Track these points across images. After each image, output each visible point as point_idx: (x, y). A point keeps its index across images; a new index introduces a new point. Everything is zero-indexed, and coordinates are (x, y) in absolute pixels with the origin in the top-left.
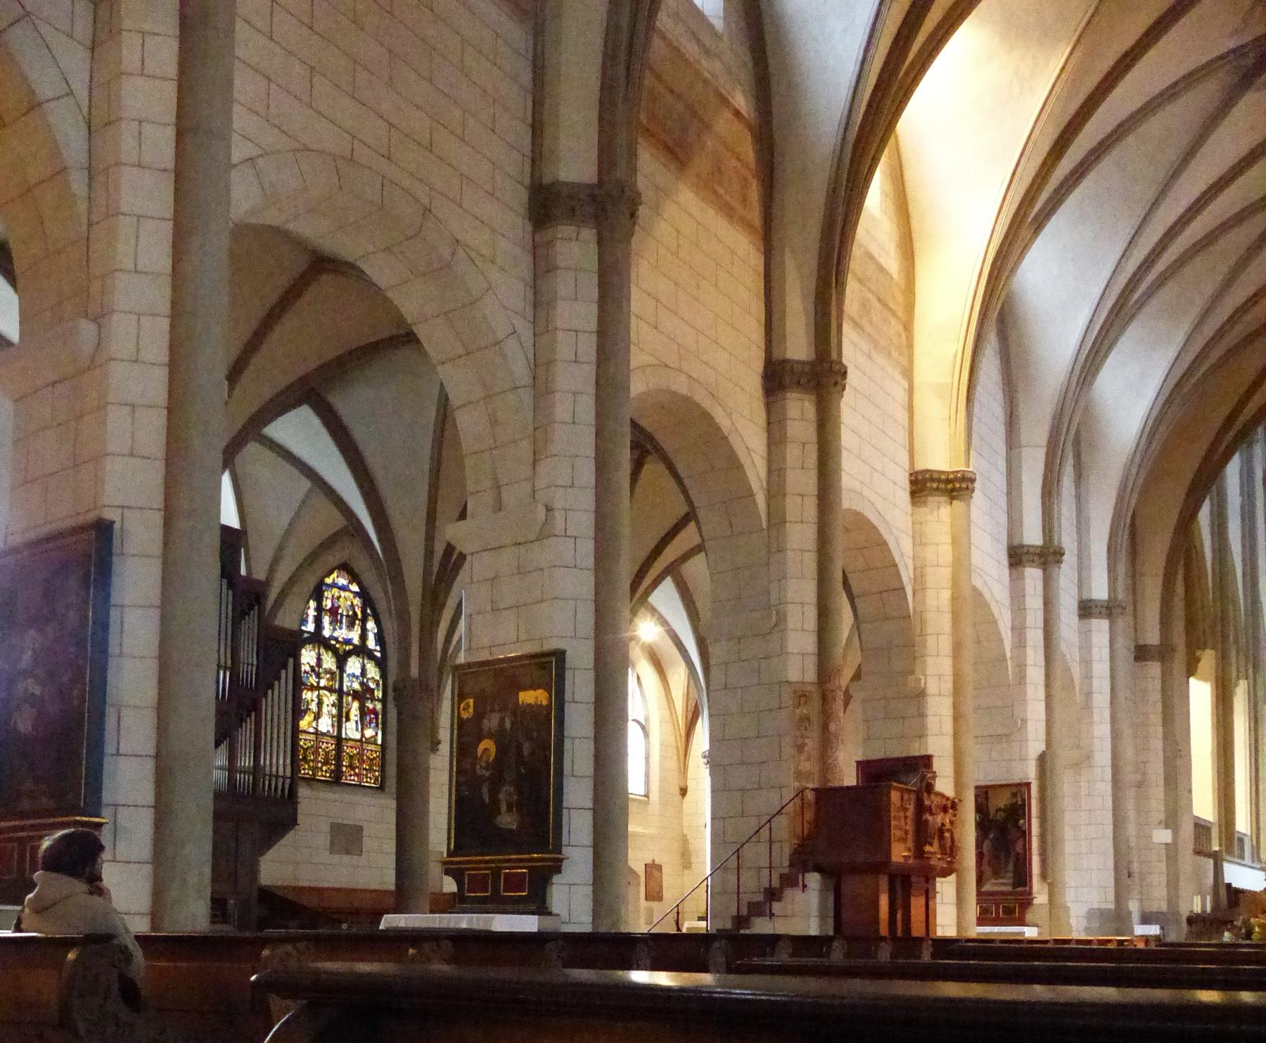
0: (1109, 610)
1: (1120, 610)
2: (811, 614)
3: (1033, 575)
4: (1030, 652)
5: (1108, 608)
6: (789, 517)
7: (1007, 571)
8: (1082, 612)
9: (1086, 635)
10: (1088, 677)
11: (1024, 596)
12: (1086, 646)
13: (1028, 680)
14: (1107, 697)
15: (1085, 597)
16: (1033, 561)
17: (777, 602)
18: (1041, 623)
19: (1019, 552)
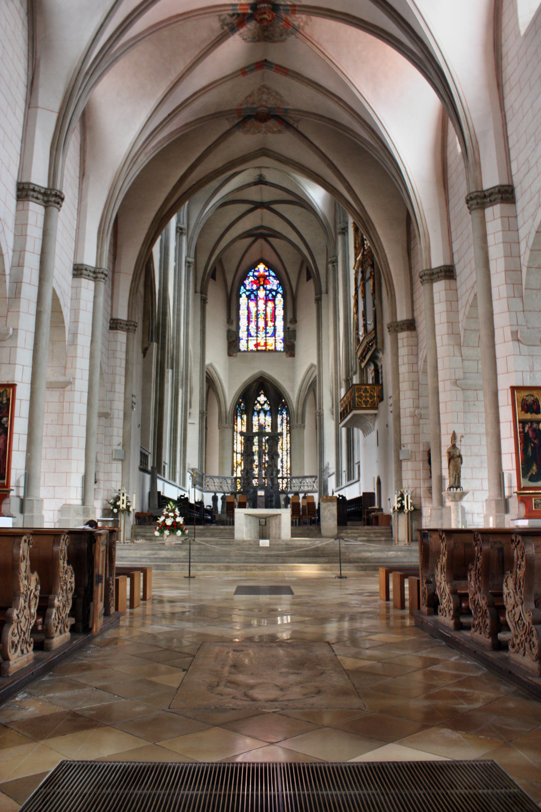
1: (103, 276)
4: (26, 271)
5: (94, 272)
7: (14, 201)
8: (75, 272)
9: (76, 290)
10: (76, 321)
11: (27, 224)
12: (76, 298)
15: (79, 262)
16: (37, 198)
18: (38, 250)
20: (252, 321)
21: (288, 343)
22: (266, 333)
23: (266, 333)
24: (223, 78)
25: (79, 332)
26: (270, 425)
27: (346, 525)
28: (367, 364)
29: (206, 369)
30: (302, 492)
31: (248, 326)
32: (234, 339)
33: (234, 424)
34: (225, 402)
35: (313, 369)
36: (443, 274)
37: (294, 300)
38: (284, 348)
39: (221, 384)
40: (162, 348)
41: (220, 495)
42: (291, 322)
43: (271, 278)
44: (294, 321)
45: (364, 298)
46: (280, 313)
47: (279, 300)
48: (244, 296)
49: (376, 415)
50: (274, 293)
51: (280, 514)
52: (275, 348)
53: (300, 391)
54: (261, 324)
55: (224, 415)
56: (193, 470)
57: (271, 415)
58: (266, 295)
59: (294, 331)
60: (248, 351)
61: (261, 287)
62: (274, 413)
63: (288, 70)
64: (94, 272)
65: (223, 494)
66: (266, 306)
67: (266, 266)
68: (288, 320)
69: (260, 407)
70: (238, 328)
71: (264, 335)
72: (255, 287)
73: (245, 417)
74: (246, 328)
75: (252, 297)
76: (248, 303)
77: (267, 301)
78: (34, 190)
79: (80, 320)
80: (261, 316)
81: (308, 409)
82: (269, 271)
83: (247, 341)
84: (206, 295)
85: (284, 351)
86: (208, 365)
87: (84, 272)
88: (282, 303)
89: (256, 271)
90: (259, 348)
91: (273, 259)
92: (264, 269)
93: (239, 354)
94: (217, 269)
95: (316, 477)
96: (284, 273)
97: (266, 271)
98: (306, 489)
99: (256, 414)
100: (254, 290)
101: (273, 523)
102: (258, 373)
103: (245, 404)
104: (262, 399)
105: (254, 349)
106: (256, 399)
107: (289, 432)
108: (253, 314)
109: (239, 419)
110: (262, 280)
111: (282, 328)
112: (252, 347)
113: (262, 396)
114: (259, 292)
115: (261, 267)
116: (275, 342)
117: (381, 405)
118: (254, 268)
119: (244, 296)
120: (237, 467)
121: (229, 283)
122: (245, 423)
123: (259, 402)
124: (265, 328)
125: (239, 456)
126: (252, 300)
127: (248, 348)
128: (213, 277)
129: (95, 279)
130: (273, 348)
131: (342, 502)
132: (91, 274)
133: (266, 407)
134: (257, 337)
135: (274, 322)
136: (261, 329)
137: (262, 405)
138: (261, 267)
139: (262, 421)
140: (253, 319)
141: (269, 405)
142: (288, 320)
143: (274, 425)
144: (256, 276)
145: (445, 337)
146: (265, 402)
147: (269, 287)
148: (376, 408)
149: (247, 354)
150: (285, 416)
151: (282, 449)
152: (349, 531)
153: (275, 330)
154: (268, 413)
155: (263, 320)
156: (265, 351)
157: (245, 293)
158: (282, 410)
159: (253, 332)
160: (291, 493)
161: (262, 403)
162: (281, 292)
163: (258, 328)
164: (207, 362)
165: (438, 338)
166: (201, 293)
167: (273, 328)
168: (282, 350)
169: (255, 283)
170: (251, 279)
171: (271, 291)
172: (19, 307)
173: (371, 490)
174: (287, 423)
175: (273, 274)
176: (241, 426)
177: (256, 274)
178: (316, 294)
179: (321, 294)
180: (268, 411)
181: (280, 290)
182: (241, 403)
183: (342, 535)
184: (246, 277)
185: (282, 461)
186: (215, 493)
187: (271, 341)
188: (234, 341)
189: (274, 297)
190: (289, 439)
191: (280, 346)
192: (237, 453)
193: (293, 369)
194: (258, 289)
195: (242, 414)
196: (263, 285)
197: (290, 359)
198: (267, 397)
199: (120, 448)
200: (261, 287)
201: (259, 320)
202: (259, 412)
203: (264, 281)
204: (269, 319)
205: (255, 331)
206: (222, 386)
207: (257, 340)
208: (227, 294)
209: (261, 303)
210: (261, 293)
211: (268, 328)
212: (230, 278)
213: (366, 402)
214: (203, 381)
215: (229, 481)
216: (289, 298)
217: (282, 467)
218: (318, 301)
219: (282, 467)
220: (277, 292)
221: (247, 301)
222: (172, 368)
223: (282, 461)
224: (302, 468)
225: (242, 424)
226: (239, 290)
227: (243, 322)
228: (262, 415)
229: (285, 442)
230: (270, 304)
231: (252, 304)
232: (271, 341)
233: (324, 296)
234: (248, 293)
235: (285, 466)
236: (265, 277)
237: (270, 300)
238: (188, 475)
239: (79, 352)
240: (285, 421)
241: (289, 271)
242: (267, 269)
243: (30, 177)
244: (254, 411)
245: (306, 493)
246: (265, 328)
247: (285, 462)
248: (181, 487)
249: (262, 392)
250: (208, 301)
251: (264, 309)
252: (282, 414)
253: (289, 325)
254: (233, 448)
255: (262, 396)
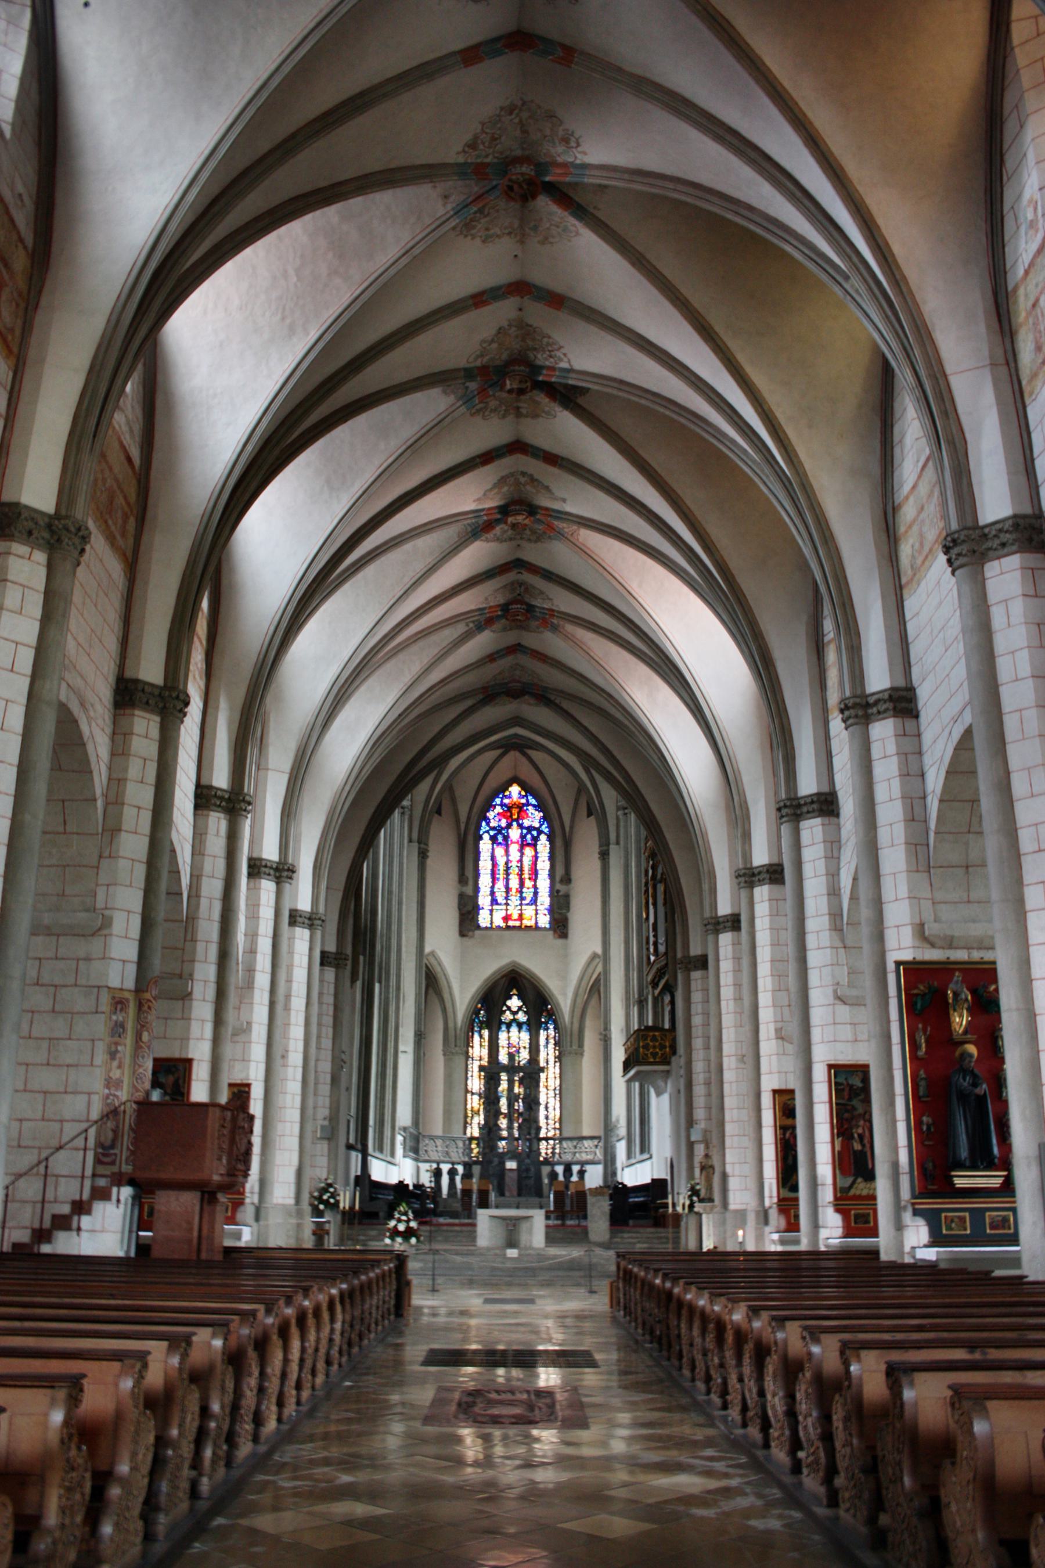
0: (311, 921)
1: (319, 922)
2: (136, 922)
3: (267, 887)
4: (259, 958)
5: (310, 919)
6: (124, 827)
11: (259, 905)
13: (256, 985)
14: (303, 1002)
16: (269, 875)
17: (103, 906)
19: (258, 863)
20: (498, 879)
21: (556, 916)
22: (522, 898)
23: (522, 898)
24: (467, 667)
25: (293, 993)
26: (527, 1046)
27: (627, 1225)
28: (662, 992)
29: (425, 961)
30: (576, 1163)
31: (493, 887)
32: (469, 908)
33: (468, 1046)
34: (454, 1013)
35: (597, 960)
36: (729, 924)
37: (568, 845)
38: (550, 923)
39: (448, 982)
40: (371, 963)
41: (445, 1168)
42: (561, 881)
43: (530, 808)
44: (567, 879)
45: (655, 904)
46: (544, 865)
47: (544, 845)
48: (486, 837)
49: (668, 1072)
50: (535, 833)
51: (532, 1217)
52: (536, 923)
53: (576, 994)
54: (514, 883)
55: (451, 1032)
56: (405, 1129)
57: (529, 1030)
58: (523, 837)
59: (567, 897)
60: (491, 928)
61: (515, 824)
62: (534, 1026)
63: (546, 656)
64: (310, 919)
65: (449, 1166)
66: (522, 854)
67: (523, 788)
68: (558, 878)
69: (512, 1017)
70: (477, 890)
71: (519, 902)
72: (504, 823)
73: (486, 1033)
74: (488, 890)
75: (500, 839)
76: (493, 849)
77: (523, 845)
78: (266, 866)
79: (294, 979)
80: (514, 870)
81: (589, 1023)
82: (526, 796)
83: (491, 911)
84: (427, 845)
85: (550, 929)
86: (429, 954)
87: (299, 919)
88: (548, 850)
89: (506, 797)
90: (511, 923)
91: (535, 781)
92: (520, 793)
93: (477, 932)
94: (444, 802)
95: (598, 1138)
96: (550, 802)
97: (523, 797)
98: (585, 1157)
99: (504, 1028)
100: (503, 829)
101: (524, 1226)
102: (507, 965)
103: (486, 1011)
104: (514, 1003)
105: (503, 925)
106: (505, 1004)
107: (559, 1058)
108: (501, 868)
109: (476, 1037)
110: (515, 811)
111: (548, 890)
112: (498, 921)
113: (515, 999)
114: (510, 831)
115: (515, 790)
116: (537, 914)
117: (674, 1059)
118: (504, 792)
119: (486, 837)
120: (472, 1117)
121: (463, 818)
122: (486, 1044)
123: (509, 1008)
124: (520, 891)
125: (476, 1098)
126: (499, 844)
127: (491, 923)
128: (439, 812)
129: (311, 927)
130: (532, 923)
131: (618, 1193)
132: (306, 921)
133: (522, 1017)
134: (507, 904)
135: (535, 881)
136: (513, 892)
137: (514, 1013)
138: (515, 790)
139: (514, 1040)
140: (501, 875)
141: (525, 1012)
142: (558, 878)
143: (534, 1049)
144: (505, 805)
145: (731, 1003)
146: (520, 1008)
147: (526, 823)
148: (668, 1063)
149: (491, 932)
150: (551, 1032)
151: (547, 1087)
152: (626, 1235)
153: (536, 894)
154: (524, 1027)
155: (517, 877)
156: (520, 927)
157: (487, 832)
158: (546, 1023)
159: (500, 897)
160: (559, 1163)
161: (515, 1009)
162: (546, 831)
163: (508, 889)
164: (428, 949)
165: (723, 1004)
166: (419, 842)
167: (533, 890)
168: (548, 926)
169: (505, 817)
170: (498, 809)
171: (530, 829)
172: (252, 998)
173: (663, 1176)
174: (555, 1044)
175: (533, 801)
176: (479, 1050)
177: (506, 801)
178: (601, 846)
179: (608, 844)
180: (524, 1023)
181: (545, 828)
182: (480, 1010)
183: (616, 1240)
184: (490, 806)
185: (547, 1108)
186: (438, 1164)
187: (529, 911)
188: (469, 912)
189: (536, 839)
190: (557, 1070)
191: (544, 921)
192: (473, 1094)
193: (565, 957)
194: (509, 826)
195: (481, 1028)
196: (517, 820)
197: (560, 942)
198: (523, 1001)
199: (326, 1123)
200: (515, 824)
201: (511, 877)
202: (509, 1026)
203: (519, 813)
204: (526, 876)
205: (504, 895)
206: (450, 987)
207: (507, 910)
208: (459, 834)
209: (514, 849)
210: (515, 833)
211: (524, 890)
212: (463, 810)
213: (654, 1055)
214: (420, 983)
215: (460, 1144)
216: (559, 842)
217: (547, 1118)
218: (604, 855)
219: (547, 1118)
220: (540, 832)
221: (490, 846)
222: (380, 982)
223: (547, 1108)
224: (579, 1122)
225: (481, 1045)
226: (479, 827)
227: (485, 881)
228: (514, 1029)
229: (551, 1076)
230: (529, 852)
231: (499, 851)
232: (529, 911)
233: (613, 849)
234: (492, 833)
235: (551, 1116)
236: (521, 808)
237: (528, 845)
238: (399, 1139)
239: (293, 1020)
240: (552, 1041)
241: (559, 798)
242: (523, 793)
243: (261, 850)
244: (501, 1023)
245: (582, 1164)
246: (520, 891)
247: (550, 1109)
248: (389, 1159)
249: (514, 991)
250: (429, 854)
251: (518, 858)
252: (547, 1029)
253: (558, 886)
254: (466, 1085)
255: (515, 999)
